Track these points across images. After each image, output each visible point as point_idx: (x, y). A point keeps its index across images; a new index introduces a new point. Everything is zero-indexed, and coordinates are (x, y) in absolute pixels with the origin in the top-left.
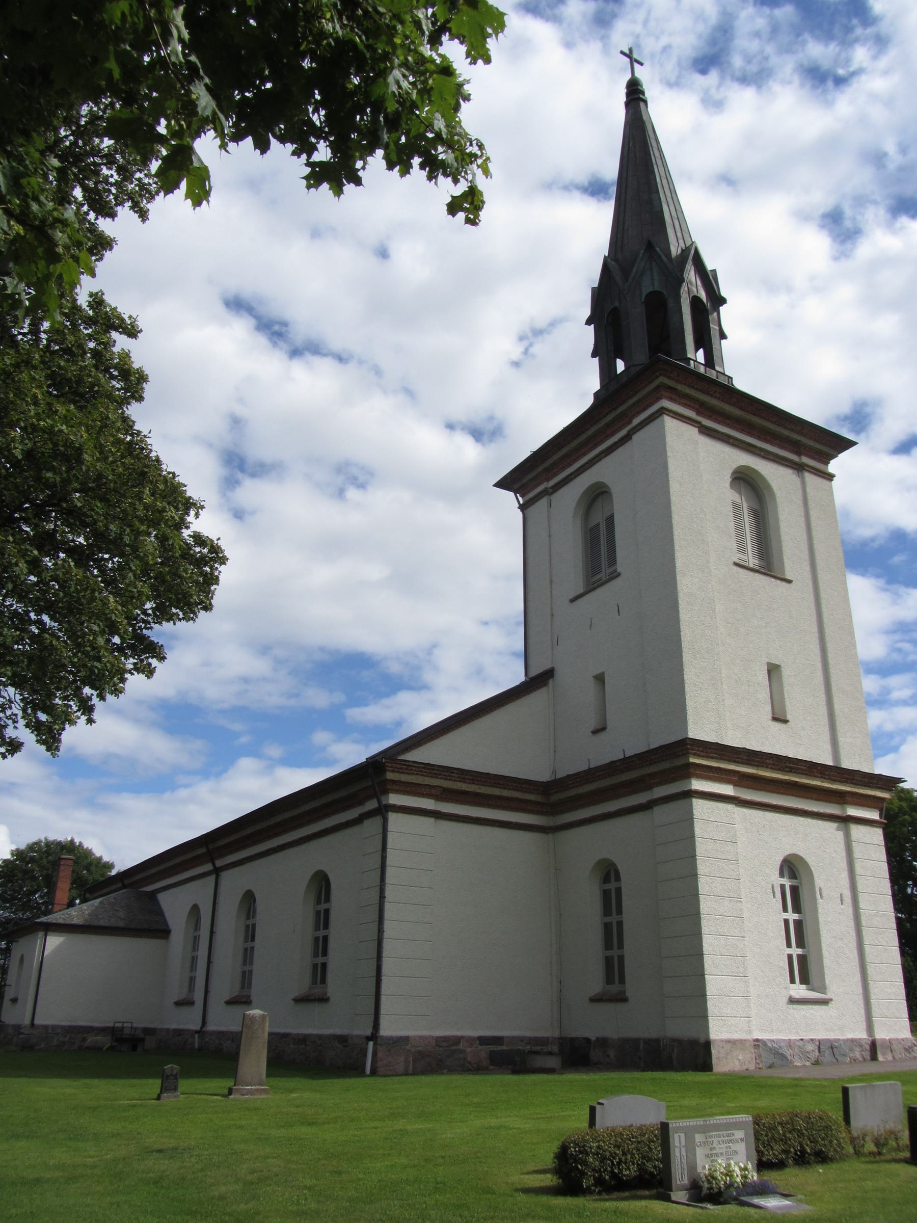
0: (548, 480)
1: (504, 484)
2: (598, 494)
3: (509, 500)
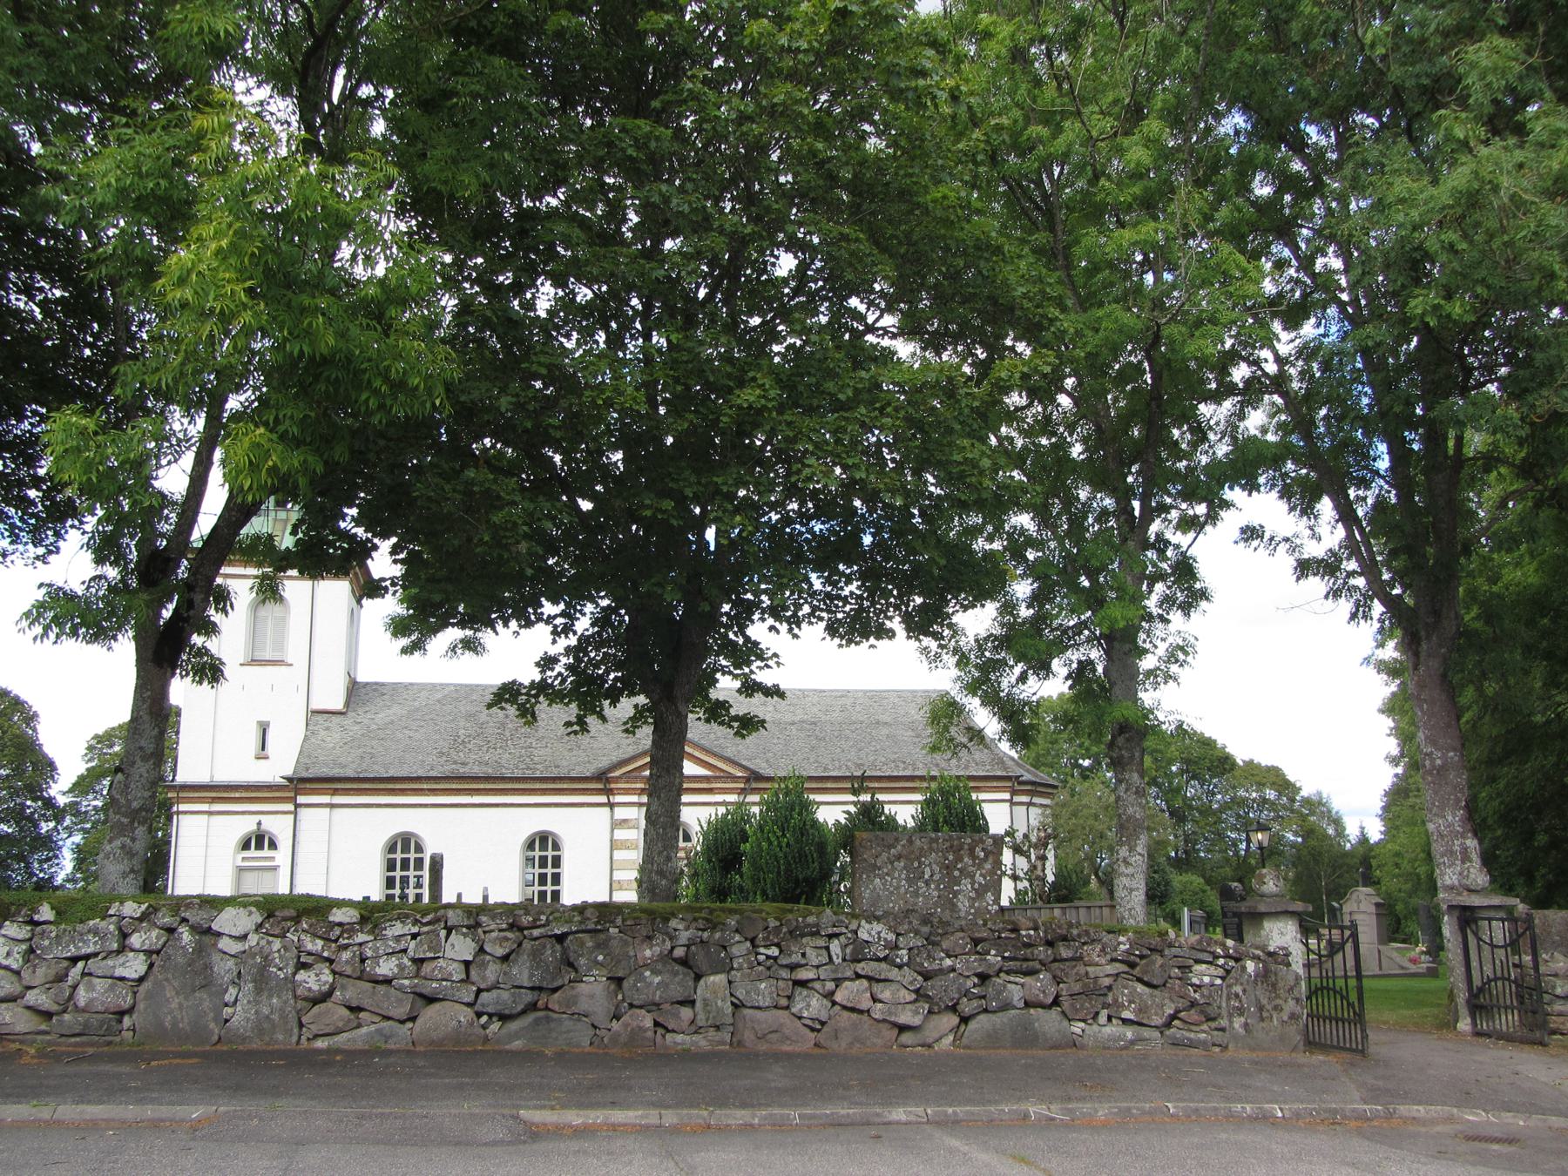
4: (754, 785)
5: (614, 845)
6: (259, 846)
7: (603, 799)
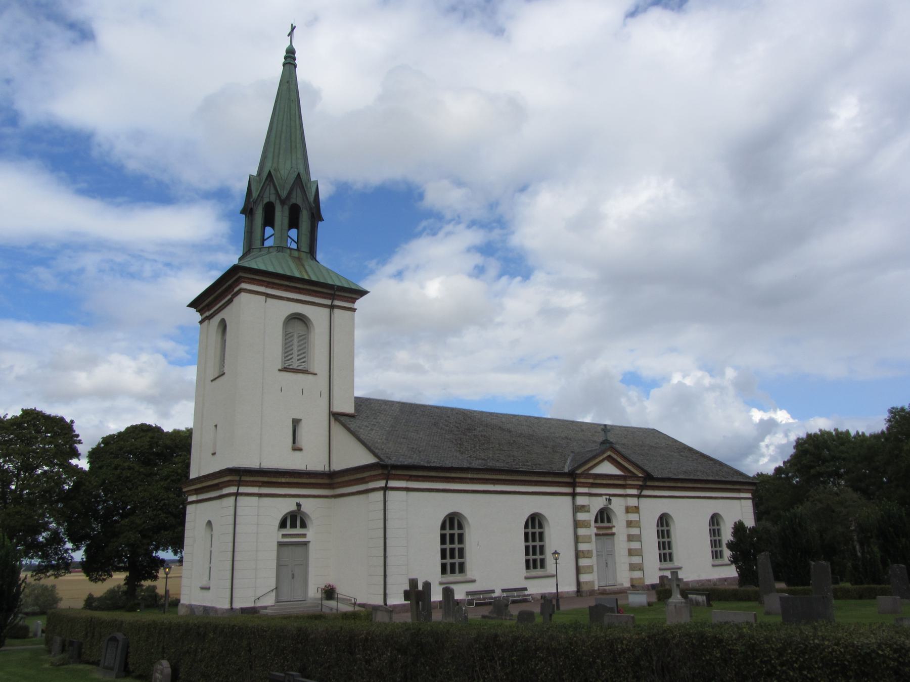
0: (209, 310)
1: (191, 305)
2: (223, 325)
3: (195, 316)
4: (649, 483)
5: (577, 524)
6: (293, 526)
7: (568, 490)
